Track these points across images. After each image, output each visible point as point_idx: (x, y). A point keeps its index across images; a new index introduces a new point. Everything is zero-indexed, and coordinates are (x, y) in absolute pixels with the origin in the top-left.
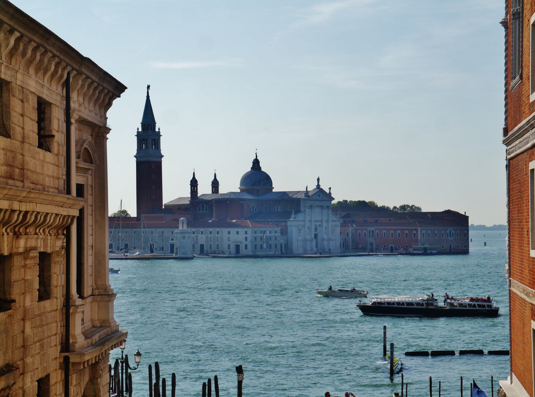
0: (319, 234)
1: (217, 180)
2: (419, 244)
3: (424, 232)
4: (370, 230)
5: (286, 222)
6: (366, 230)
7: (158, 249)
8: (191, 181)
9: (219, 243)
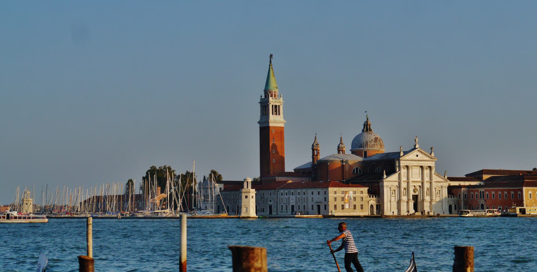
1: (342, 144)
2: (525, 205)
3: (530, 192)
4: (481, 192)
5: (379, 182)
6: (478, 191)
7: (260, 210)
8: (313, 146)
9: (305, 204)
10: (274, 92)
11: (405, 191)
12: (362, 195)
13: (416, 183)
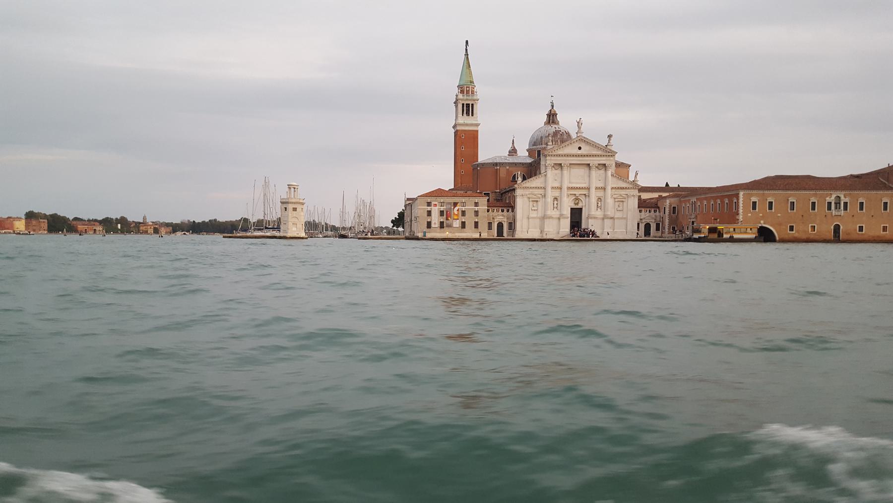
0: (584, 209)
3: (754, 199)
4: (692, 202)
5: (514, 190)
10: (467, 87)
11: (556, 202)
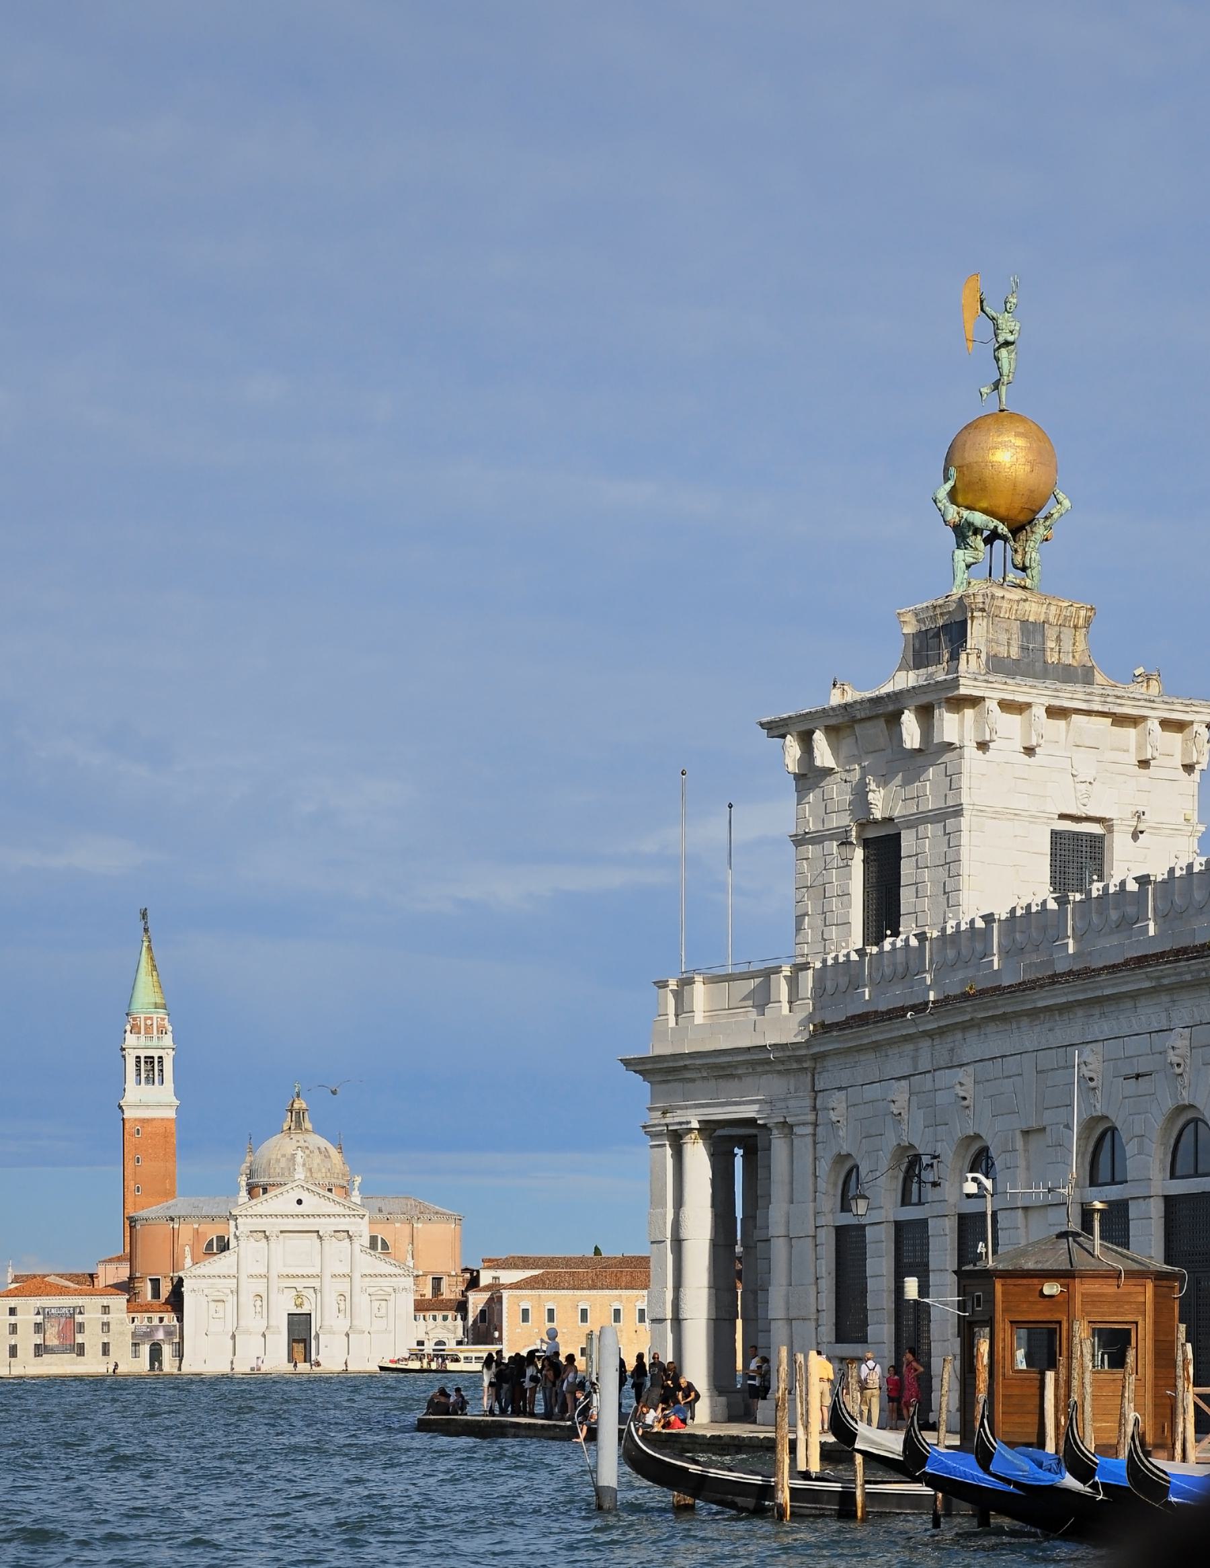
3: (525, 1305)
10: (146, 1019)
11: (259, 1303)
12: (105, 1318)
13: (300, 1280)
